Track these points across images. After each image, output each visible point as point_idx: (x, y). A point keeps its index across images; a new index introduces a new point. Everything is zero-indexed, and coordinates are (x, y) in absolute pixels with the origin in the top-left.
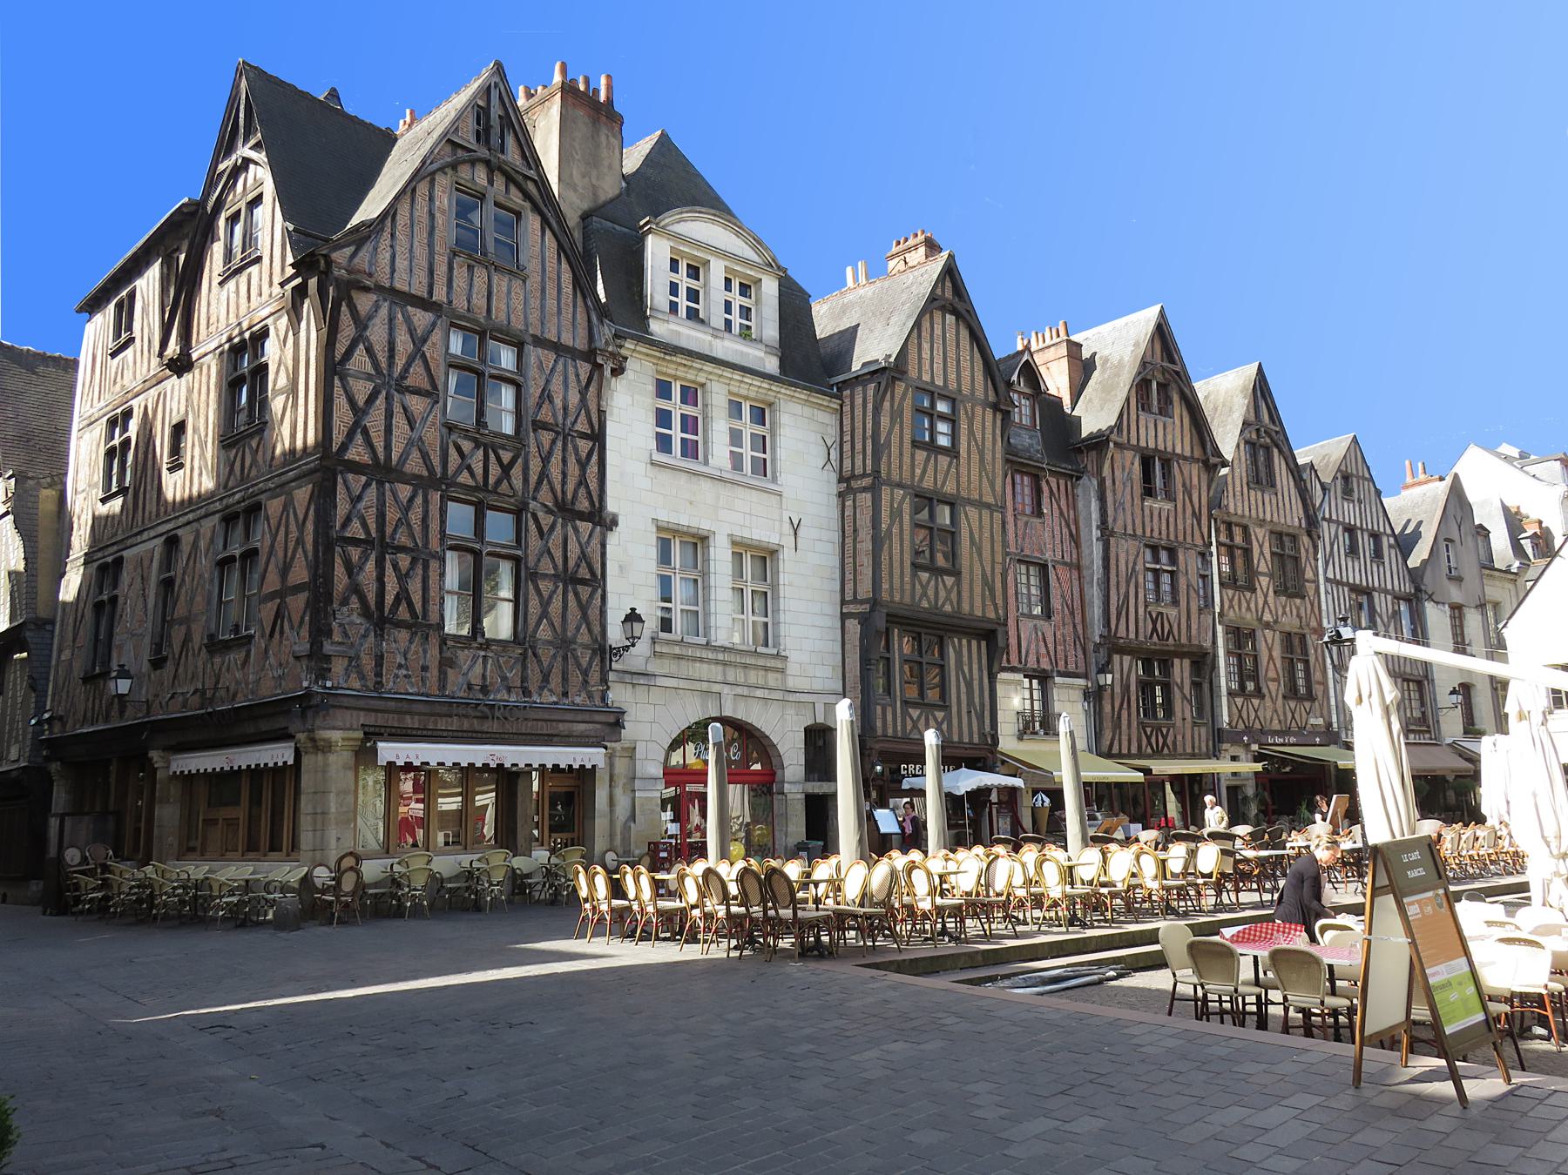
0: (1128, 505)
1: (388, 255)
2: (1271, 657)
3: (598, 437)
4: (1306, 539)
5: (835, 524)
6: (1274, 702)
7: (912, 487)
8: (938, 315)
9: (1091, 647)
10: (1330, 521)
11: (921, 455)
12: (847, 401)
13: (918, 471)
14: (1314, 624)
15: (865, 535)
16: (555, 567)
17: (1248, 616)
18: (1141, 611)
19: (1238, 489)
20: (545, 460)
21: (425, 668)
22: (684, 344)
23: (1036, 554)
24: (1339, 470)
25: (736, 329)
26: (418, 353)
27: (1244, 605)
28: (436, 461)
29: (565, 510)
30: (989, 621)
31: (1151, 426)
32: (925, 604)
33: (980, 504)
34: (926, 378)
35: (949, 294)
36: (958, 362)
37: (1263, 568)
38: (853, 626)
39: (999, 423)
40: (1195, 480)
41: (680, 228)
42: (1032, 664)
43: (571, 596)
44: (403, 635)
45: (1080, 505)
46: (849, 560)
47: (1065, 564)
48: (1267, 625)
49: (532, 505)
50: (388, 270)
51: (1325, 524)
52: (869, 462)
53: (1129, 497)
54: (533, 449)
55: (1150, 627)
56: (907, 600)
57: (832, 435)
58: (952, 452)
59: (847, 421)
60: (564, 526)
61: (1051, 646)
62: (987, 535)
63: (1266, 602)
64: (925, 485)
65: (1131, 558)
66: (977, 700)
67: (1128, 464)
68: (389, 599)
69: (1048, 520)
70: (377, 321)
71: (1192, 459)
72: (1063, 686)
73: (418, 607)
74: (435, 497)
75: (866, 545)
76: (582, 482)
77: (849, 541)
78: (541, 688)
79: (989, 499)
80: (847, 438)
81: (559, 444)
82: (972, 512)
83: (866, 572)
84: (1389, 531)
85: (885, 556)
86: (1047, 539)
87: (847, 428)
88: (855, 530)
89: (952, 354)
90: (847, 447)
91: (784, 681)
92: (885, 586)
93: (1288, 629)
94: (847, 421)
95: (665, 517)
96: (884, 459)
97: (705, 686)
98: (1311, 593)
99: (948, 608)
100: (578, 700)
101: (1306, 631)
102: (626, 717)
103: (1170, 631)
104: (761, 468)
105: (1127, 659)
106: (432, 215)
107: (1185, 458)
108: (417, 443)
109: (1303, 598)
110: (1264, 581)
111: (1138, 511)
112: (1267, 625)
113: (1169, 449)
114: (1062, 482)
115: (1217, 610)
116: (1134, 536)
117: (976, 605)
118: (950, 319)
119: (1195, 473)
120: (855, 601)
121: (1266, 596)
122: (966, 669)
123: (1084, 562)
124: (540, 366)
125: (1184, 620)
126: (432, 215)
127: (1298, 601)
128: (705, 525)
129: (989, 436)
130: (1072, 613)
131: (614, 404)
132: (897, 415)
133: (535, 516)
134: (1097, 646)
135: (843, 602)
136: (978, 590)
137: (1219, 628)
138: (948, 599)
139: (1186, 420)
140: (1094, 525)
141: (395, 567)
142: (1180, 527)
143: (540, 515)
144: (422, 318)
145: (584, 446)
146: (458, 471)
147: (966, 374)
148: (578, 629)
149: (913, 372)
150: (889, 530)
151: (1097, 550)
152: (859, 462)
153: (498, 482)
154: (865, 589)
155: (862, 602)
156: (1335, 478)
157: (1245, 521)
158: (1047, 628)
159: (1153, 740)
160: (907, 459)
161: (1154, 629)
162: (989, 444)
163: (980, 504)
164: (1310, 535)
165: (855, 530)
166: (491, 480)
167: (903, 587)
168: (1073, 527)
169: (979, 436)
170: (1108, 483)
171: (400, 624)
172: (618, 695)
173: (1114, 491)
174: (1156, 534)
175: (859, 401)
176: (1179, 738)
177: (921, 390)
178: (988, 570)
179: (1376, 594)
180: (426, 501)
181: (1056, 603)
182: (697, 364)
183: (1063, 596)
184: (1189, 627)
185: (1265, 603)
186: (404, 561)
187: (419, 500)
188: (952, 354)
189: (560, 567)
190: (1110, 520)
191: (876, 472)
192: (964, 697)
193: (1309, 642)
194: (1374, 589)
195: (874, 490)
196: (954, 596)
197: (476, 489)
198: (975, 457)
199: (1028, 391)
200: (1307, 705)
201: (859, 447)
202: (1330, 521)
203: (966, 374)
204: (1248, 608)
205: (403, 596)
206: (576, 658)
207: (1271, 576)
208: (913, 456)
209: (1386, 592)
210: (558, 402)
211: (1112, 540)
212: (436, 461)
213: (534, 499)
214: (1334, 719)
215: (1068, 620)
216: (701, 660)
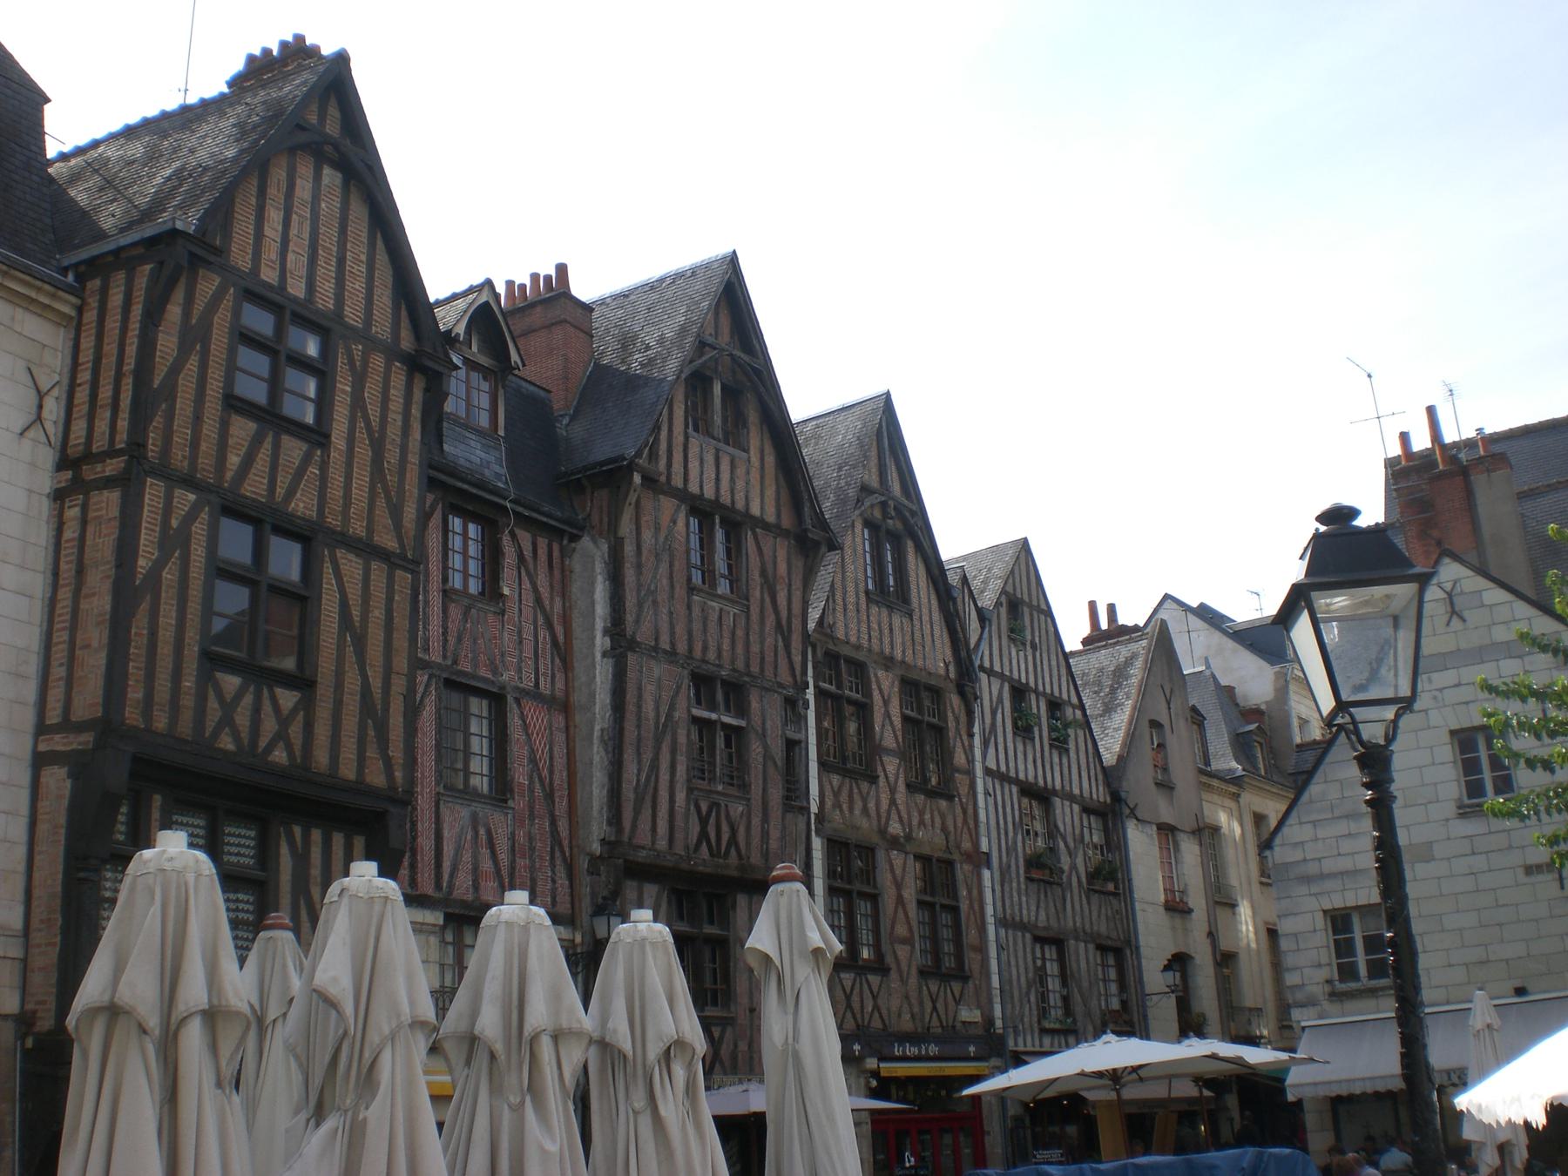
0: (662, 597)
2: (900, 900)
4: (955, 700)
5: (40, 557)
6: (904, 981)
8: (305, 169)
9: (583, 863)
10: (990, 672)
11: (241, 429)
12: (93, 302)
13: (234, 460)
14: (966, 845)
15: (100, 584)
17: (864, 823)
18: (681, 797)
19: (851, 599)
23: (483, 672)
24: (1003, 592)
27: (859, 805)
30: (372, 792)
31: (709, 458)
32: (227, 743)
33: (367, 550)
34: (269, 275)
35: (332, 128)
36: (341, 261)
37: (889, 741)
38: (57, 780)
39: (418, 395)
40: (782, 568)
45: (576, 588)
46: (61, 637)
48: (894, 843)
51: (983, 677)
52: (123, 424)
53: (665, 582)
55: (695, 829)
56: (185, 728)
57: (54, 365)
58: (317, 436)
59: (87, 343)
61: (504, 857)
62: (378, 613)
63: (893, 802)
65: (666, 696)
67: (665, 520)
69: (512, 609)
71: (775, 530)
75: (99, 602)
77: (65, 594)
79: (389, 542)
80: (85, 376)
82: (351, 565)
83: (94, 663)
84: (1075, 700)
86: (509, 648)
87: (86, 356)
88: (80, 571)
90: (82, 395)
92: (135, 694)
93: (926, 851)
94: (87, 343)
96: (158, 421)
98: (963, 790)
99: (279, 756)
101: (956, 856)
103: (733, 839)
107: (766, 526)
109: (950, 798)
110: (891, 765)
111: (681, 609)
112: (894, 843)
113: (740, 505)
115: (814, 808)
116: (672, 654)
117: (343, 754)
118: (330, 176)
119: (782, 555)
120: (67, 725)
121: (893, 791)
123: (578, 698)
125: (756, 821)
127: (943, 803)
129: (395, 418)
130: (550, 796)
132: (195, 337)
134: (595, 861)
135: (41, 729)
136: (350, 724)
137: (817, 844)
138: (281, 736)
139: (770, 459)
140: (599, 625)
142: (755, 648)
147: (356, 286)
149: (240, 257)
150: (155, 574)
151: (602, 673)
152: (102, 426)
154: (89, 701)
155: (80, 727)
156: (998, 604)
157: (861, 656)
158: (501, 825)
160: (210, 428)
161: (703, 834)
163: (367, 550)
164: (962, 693)
165: (80, 571)
167: (177, 700)
168: (559, 630)
169: (374, 411)
170: (629, 549)
174: (711, 656)
175: (116, 298)
176: (743, 1046)
178: (376, 684)
179: (1057, 801)
181: (520, 774)
183: (533, 761)
184: (765, 835)
185: (889, 802)
190: (630, 618)
191: (136, 447)
193: (960, 876)
194: (1054, 792)
195: (128, 484)
196: (296, 731)
198: (364, 452)
199: (484, 360)
200: (956, 987)
201: (106, 393)
202: (990, 672)
203: (356, 286)
204: (865, 810)
207: (902, 755)
208: (224, 426)
209: (1071, 798)
211: (632, 658)
214: (998, 1012)
215: (539, 807)
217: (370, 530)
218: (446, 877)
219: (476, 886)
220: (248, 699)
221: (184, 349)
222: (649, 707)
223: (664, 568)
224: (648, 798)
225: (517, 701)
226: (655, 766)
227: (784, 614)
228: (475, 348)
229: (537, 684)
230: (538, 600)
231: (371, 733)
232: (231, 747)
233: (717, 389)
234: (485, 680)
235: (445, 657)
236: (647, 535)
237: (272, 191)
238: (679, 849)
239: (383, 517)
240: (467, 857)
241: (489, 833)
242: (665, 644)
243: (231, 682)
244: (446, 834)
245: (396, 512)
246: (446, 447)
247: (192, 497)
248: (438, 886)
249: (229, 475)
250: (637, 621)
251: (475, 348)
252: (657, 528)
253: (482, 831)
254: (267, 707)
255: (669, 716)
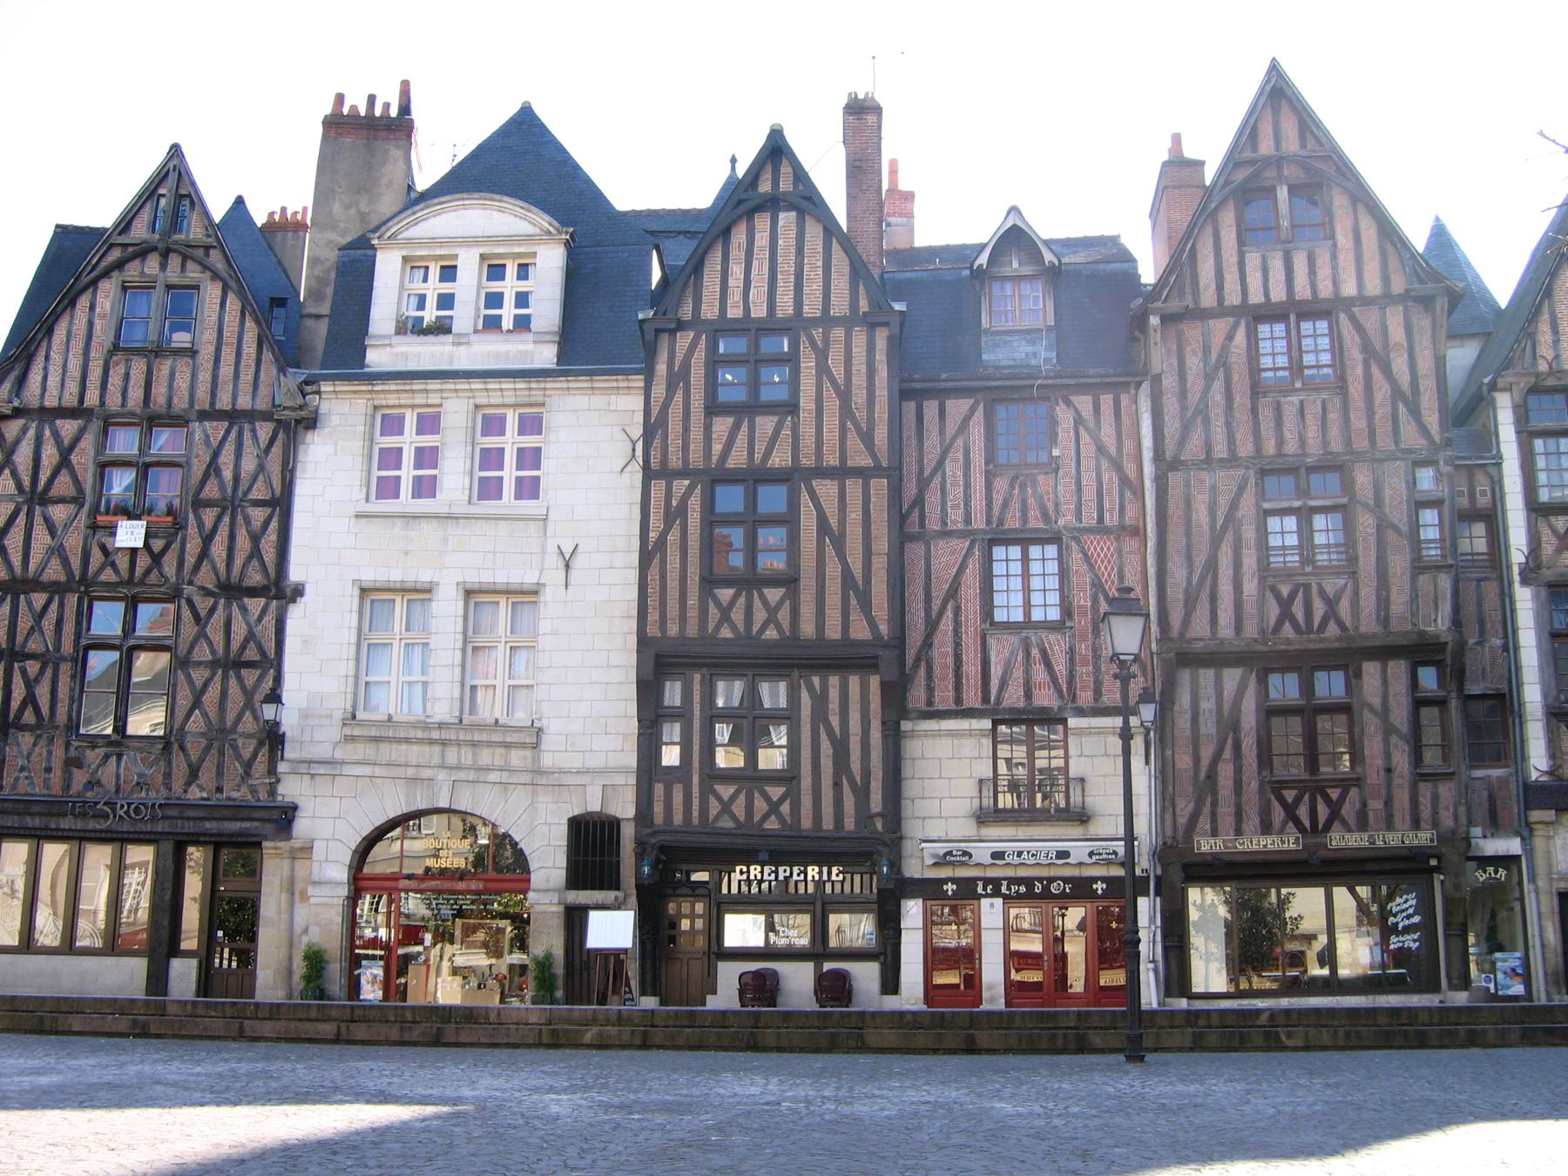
1: (39, 378)
3: (282, 504)
7: (705, 471)
11: (722, 425)
13: (717, 448)
16: (213, 652)
18: (1250, 587)
20: (208, 540)
21: (48, 770)
22: (412, 366)
25: (507, 323)
26: (64, 462)
28: (76, 563)
29: (232, 591)
33: (841, 473)
40: (1397, 334)
41: (414, 232)
42: (1014, 697)
43: (233, 682)
44: (26, 739)
47: (1101, 528)
49: (188, 590)
50: (38, 391)
54: (192, 530)
55: (1274, 611)
56: (692, 630)
60: (228, 605)
61: (1061, 668)
62: (854, 515)
64: (731, 463)
65: (1224, 501)
66: (855, 765)
68: (15, 705)
70: (24, 443)
72: (1089, 732)
73: (45, 710)
74: (72, 600)
76: (256, 552)
78: (188, 784)
79: (865, 461)
81: (227, 519)
82: (827, 489)
85: (654, 573)
89: (786, 265)
91: (536, 759)
92: (653, 616)
95: (369, 576)
97: (411, 772)
99: (771, 634)
100: (235, 794)
102: (299, 813)
104: (528, 489)
105: (1231, 677)
106: (91, 324)
108: (59, 551)
114: (1107, 400)
116: (1232, 460)
122: (835, 721)
124: (207, 442)
126: (91, 324)
128: (425, 577)
131: (310, 458)
133: (190, 603)
138: (772, 619)
141: (24, 672)
143: (197, 599)
144: (68, 427)
145: (258, 515)
146: (101, 569)
148: (239, 718)
150: (662, 541)
153: (148, 572)
159: (1303, 812)
160: (696, 433)
161: (1286, 614)
162: (859, 380)
163: (841, 473)
166: (139, 572)
169: (838, 373)
171: (23, 728)
172: (291, 789)
173: (1183, 394)
177: (722, 327)
180: (61, 605)
182: (418, 385)
186: (33, 667)
187: (54, 606)
188: (786, 265)
189: (221, 651)
192: (827, 764)
196: (784, 616)
197: (120, 584)
198: (832, 405)
199: (1027, 270)
205: (30, 699)
206: (235, 748)
210: (228, 474)
211: (1174, 478)
212: (76, 563)
213: (190, 583)
216: (407, 741)
217: (843, 458)
218: (994, 692)
219: (1028, 695)
220: (742, 601)
221: (671, 390)
222: (1201, 514)
223: (1218, 385)
224: (1204, 597)
225: (1078, 541)
226: (1212, 566)
227: (1404, 379)
228: (1015, 265)
229: (1101, 519)
230: (1101, 449)
231: (854, 602)
232: (730, 635)
233: (1283, 193)
234: (1036, 530)
235: (989, 522)
236: (1194, 363)
237: (733, 253)
238: (1251, 631)
239: (854, 442)
240: (1018, 673)
241: (1044, 653)
242: (1221, 450)
243: (726, 594)
244: (993, 659)
245: (868, 438)
246: (985, 357)
247: (687, 482)
248: (986, 699)
249: (714, 459)
250: (1183, 440)
251: (1015, 265)
252: (1207, 350)
253: (1035, 652)
254: (757, 603)
255: (1230, 518)
